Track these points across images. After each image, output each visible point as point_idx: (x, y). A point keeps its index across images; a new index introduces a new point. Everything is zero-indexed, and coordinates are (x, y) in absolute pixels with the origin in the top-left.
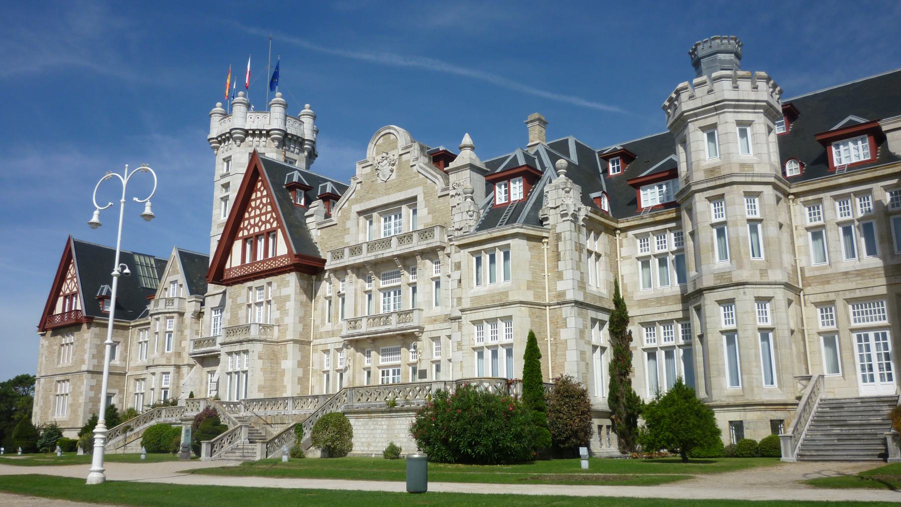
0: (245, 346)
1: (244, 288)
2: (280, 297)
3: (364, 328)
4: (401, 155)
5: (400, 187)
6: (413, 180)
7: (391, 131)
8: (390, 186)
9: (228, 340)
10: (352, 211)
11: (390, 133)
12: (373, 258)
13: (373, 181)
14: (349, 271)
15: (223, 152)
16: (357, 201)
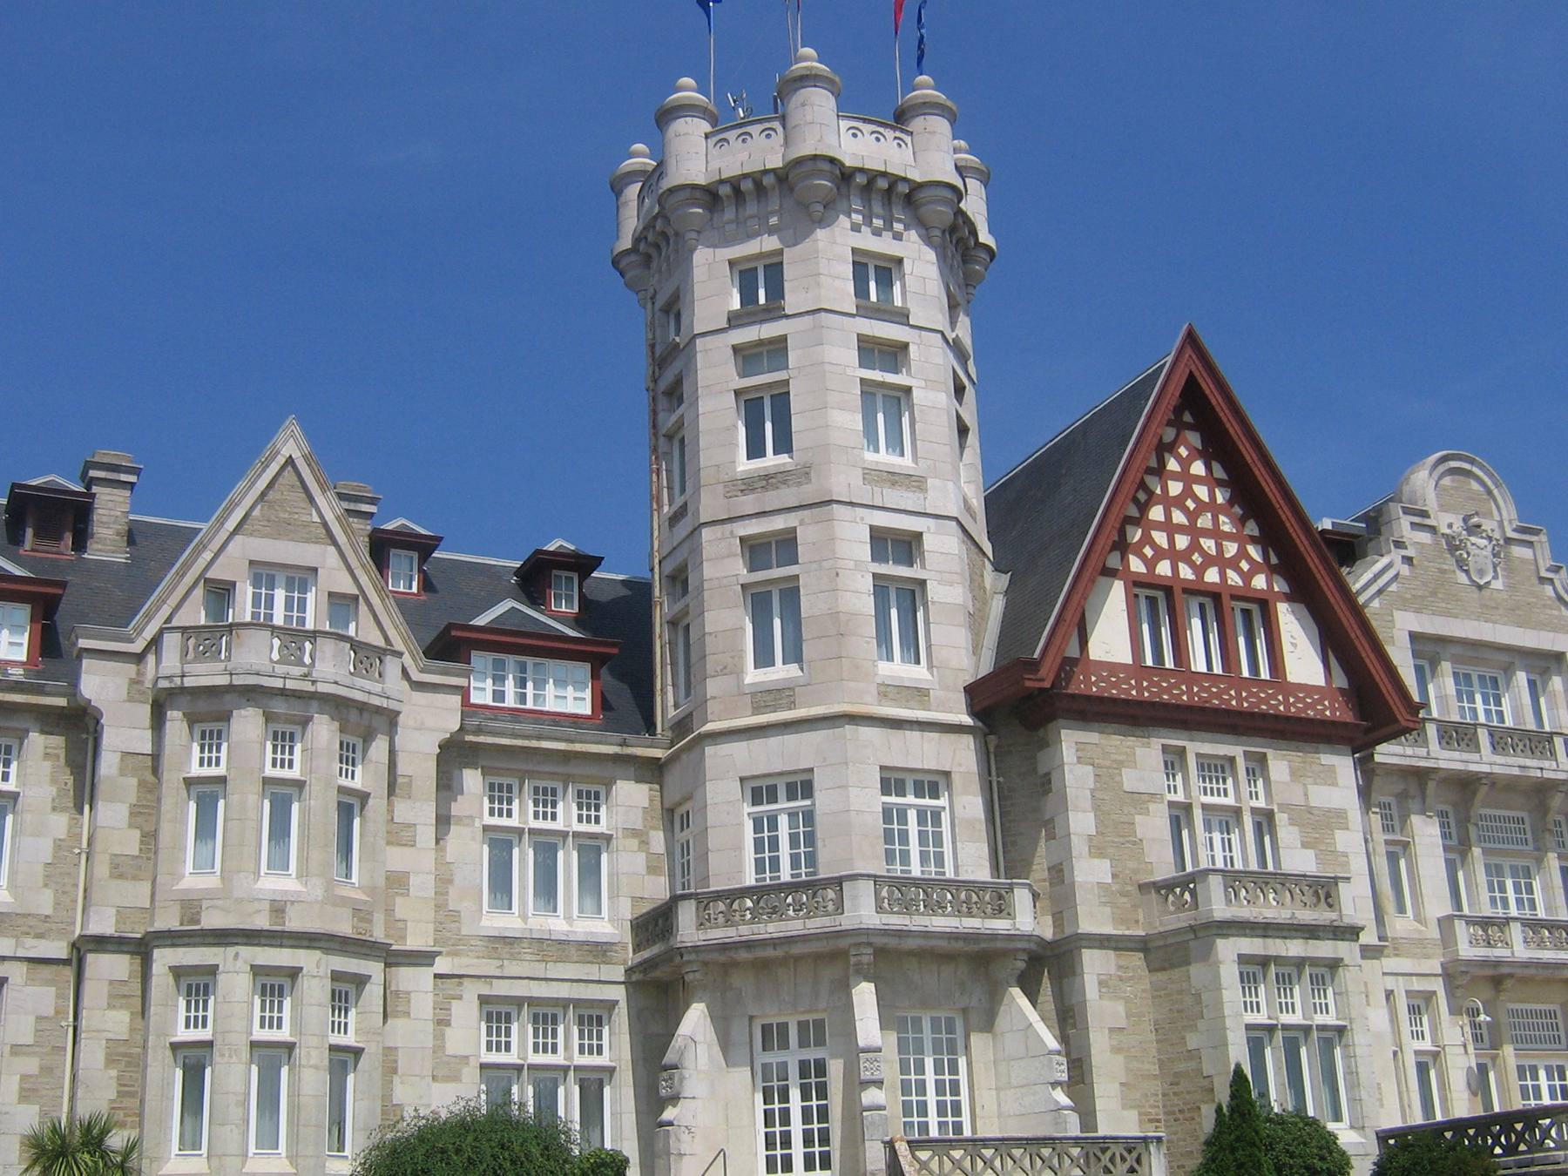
0: (1324, 949)
1: (1148, 745)
2: (1310, 810)
3: (1518, 948)
4: (1508, 541)
5: (1520, 615)
6: (1549, 611)
7: (1475, 470)
8: (1492, 604)
9: (1244, 912)
10: (1397, 626)
11: (1468, 474)
12: (1516, 771)
13: (1443, 572)
14: (1431, 785)
15: (856, 228)
16: (1405, 604)
